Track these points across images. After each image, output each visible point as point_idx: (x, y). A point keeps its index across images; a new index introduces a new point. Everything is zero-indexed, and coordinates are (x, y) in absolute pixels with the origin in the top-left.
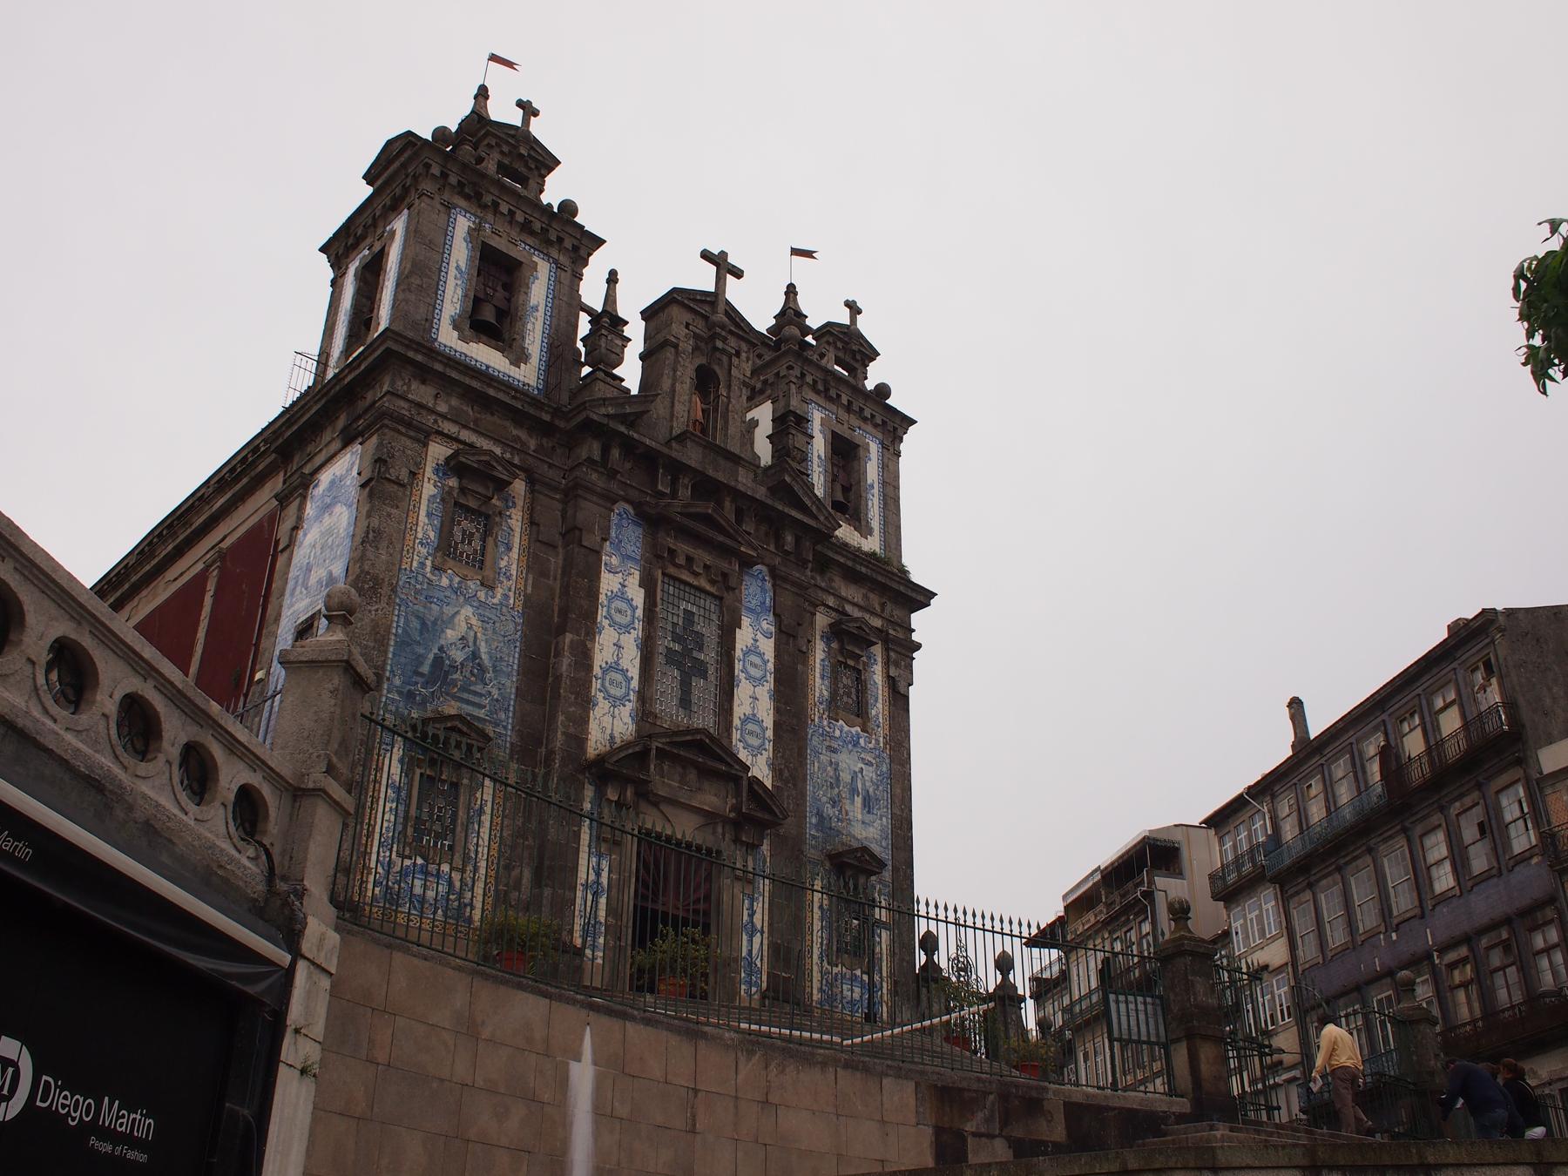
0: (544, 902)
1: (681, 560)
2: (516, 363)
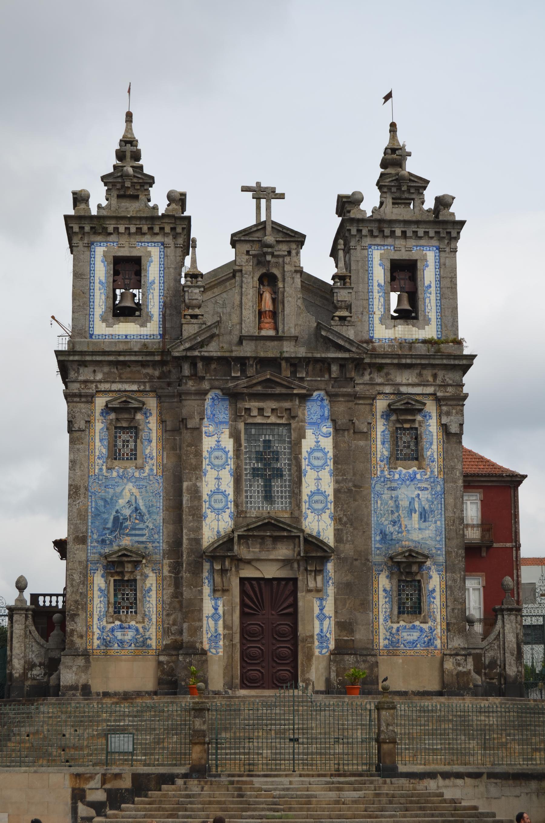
0: (184, 631)
1: (255, 413)
2: (143, 325)
